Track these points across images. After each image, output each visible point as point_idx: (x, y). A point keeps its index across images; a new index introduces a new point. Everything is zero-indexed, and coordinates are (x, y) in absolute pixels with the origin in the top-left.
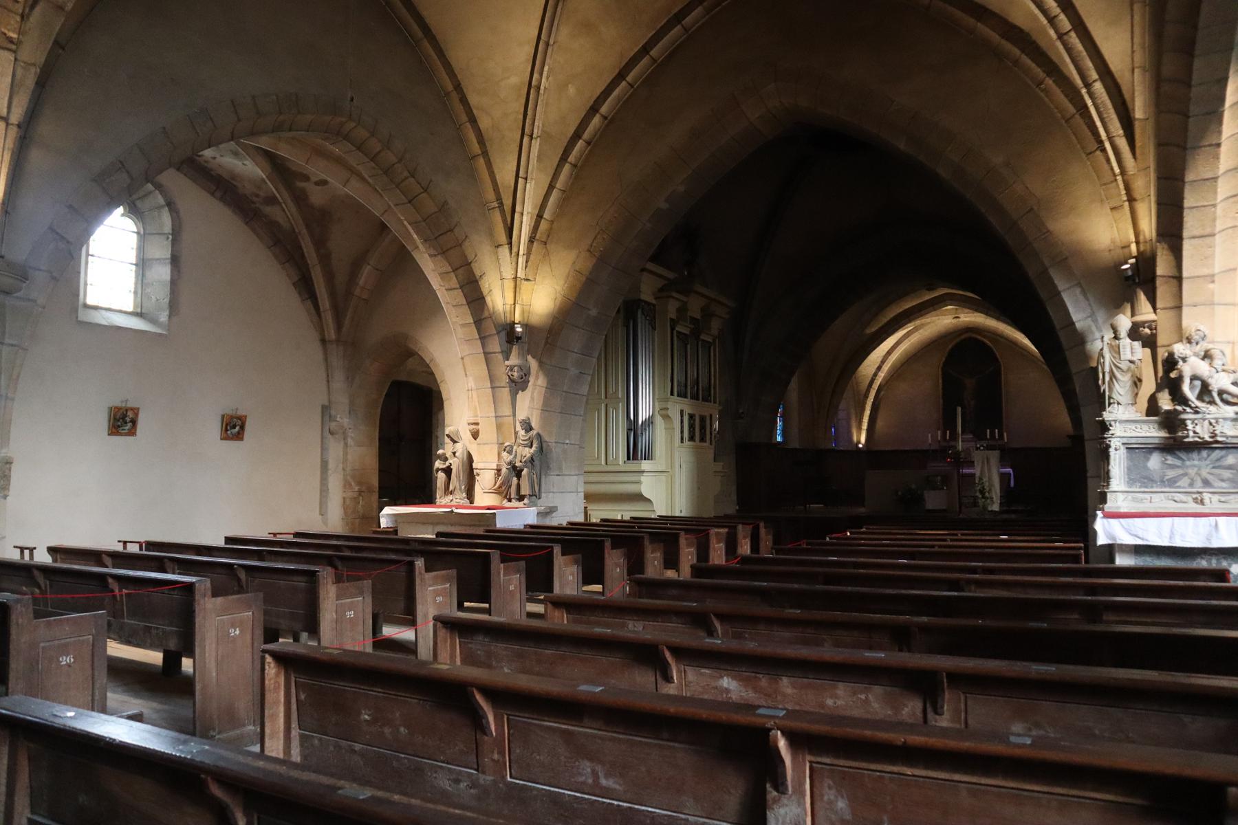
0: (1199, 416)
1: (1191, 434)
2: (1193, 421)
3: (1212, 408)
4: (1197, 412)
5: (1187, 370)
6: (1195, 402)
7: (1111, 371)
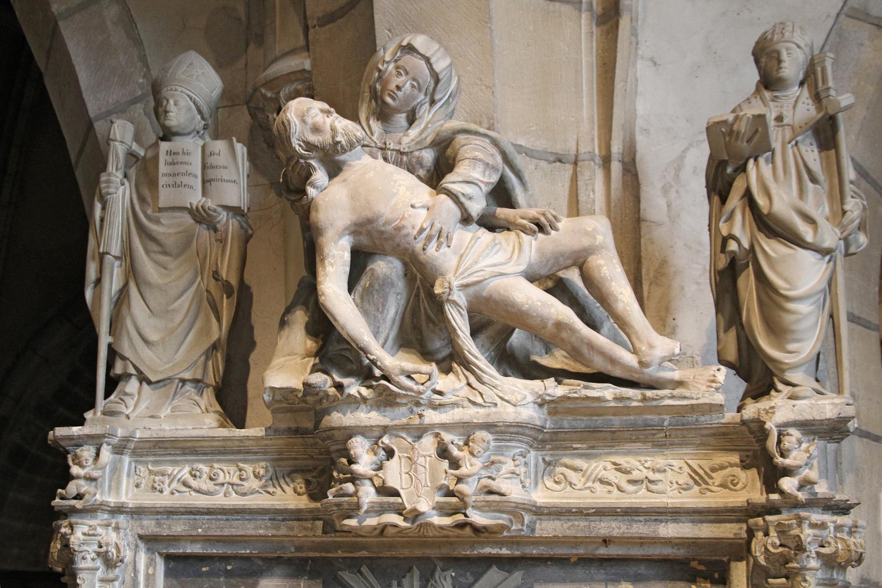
0: (398, 416)
1: (368, 495)
2: (375, 434)
3: (451, 384)
4: (386, 400)
5: (334, 202)
6: (392, 360)
7: (128, 255)
